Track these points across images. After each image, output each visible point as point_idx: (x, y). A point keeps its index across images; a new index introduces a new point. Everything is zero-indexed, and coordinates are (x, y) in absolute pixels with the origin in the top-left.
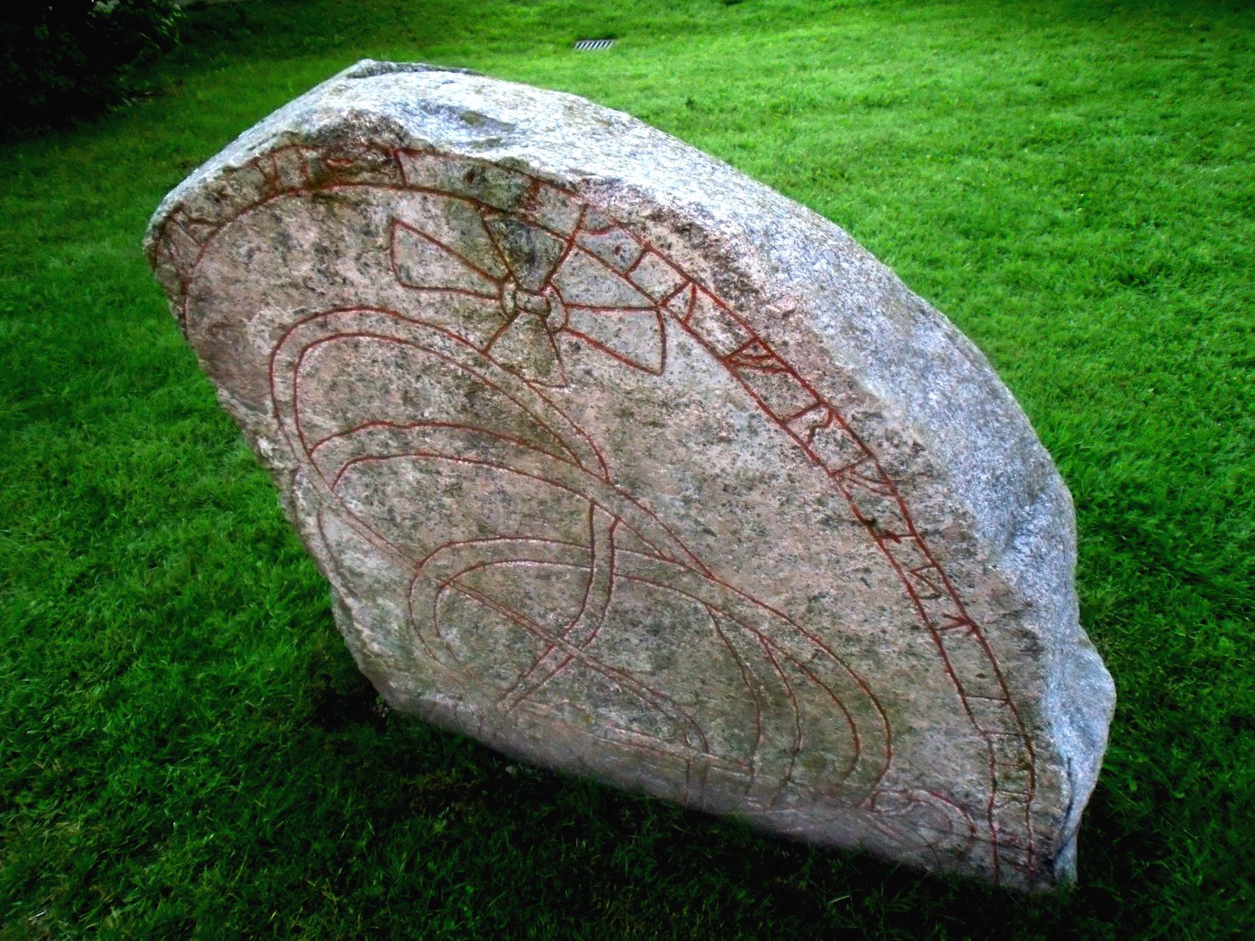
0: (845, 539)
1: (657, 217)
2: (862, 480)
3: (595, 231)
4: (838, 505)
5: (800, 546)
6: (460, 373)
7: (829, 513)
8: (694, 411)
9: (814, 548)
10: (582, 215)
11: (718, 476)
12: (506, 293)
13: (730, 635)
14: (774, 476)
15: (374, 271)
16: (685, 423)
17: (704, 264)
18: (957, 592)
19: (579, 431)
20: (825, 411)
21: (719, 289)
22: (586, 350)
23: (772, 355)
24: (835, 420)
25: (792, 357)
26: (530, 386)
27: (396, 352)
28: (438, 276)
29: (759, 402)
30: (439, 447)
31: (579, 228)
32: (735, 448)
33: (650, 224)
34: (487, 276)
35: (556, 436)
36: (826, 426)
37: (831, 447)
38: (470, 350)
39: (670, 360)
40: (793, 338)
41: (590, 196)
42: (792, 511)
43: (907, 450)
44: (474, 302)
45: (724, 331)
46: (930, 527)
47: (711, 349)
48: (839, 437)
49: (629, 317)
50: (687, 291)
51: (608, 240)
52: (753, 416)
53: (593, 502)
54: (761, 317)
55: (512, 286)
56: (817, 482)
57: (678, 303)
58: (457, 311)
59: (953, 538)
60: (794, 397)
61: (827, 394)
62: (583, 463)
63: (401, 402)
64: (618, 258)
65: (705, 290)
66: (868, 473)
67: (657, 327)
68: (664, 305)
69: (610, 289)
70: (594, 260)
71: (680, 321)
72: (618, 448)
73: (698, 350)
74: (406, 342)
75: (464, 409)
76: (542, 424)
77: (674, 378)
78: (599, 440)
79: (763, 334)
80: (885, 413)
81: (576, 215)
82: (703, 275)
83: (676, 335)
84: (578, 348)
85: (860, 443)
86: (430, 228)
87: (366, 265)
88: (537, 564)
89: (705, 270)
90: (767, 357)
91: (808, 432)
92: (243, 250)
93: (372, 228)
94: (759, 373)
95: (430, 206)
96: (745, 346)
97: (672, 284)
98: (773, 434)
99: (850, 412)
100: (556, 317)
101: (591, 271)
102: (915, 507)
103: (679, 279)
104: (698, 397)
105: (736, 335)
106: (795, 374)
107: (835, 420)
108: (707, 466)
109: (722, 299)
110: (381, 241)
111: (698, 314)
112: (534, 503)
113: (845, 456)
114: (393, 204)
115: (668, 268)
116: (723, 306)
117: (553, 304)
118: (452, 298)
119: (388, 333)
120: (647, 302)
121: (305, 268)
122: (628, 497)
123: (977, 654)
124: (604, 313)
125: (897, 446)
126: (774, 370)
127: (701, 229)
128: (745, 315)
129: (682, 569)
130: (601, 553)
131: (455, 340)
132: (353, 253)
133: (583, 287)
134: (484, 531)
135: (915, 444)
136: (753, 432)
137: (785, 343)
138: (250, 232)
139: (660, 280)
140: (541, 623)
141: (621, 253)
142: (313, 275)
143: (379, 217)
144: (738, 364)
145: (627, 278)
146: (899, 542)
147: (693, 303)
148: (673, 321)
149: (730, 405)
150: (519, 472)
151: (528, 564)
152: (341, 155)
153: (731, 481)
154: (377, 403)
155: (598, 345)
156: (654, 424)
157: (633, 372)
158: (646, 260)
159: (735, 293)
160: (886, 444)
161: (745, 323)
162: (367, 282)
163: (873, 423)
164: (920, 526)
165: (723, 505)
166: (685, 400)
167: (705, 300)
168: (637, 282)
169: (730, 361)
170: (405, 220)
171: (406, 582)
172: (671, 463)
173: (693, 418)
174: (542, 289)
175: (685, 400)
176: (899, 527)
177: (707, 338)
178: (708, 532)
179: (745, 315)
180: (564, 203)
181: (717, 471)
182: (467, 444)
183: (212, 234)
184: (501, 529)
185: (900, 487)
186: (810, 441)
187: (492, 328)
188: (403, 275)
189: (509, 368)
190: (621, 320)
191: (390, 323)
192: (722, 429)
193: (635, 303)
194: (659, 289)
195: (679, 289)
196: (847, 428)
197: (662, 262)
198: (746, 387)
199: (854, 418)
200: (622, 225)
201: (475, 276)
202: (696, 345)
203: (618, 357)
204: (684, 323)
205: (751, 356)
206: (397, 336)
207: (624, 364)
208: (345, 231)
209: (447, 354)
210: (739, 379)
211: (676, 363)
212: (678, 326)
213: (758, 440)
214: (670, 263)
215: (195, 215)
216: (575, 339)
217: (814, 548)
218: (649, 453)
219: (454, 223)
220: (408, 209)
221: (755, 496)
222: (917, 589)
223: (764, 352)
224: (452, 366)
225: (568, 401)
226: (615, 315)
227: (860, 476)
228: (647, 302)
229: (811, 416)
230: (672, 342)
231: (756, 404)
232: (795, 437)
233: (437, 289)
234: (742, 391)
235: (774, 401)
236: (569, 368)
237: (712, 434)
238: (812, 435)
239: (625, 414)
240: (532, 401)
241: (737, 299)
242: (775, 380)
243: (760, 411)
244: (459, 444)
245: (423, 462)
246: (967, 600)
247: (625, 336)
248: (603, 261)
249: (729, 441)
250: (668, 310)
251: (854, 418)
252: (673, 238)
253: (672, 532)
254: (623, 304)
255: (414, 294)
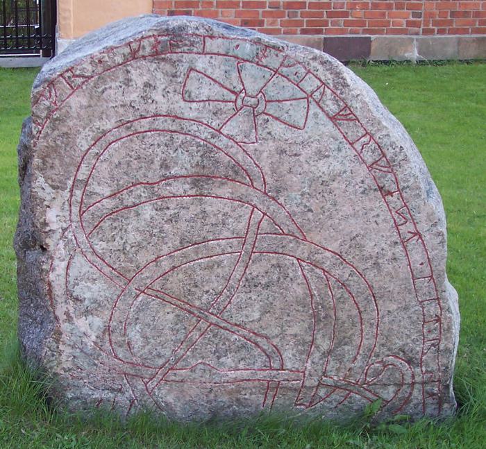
0: (370, 200)
1: (314, 59)
2: (380, 168)
3: (288, 66)
4: (370, 182)
5: (351, 208)
6: (202, 144)
7: (366, 186)
8: (315, 145)
9: (357, 208)
10: (284, 60)
11: (321, 176)
12: (239, 98)
13: (308, 276)
14: (345, 172)
15: (171, 95)
16: (310, 152)
17: (330, 76)
18: (414, 217)
19: (257, 166)
20: (368, 136)
21: (334, 86)
22: (270, 122)
23: (352, 113)
24: (372, 140)
25: (358, 114)
26: (238, 145)
27: (168, 138)
28: (206, 94)
29: (344, 136)
30: (174, 191)
31: (281, 65)
32: (331, 159)
33: (311, 62)
34: (233, 92)
35: (245, 171)
36: (368, 144)
37: (370, 154)
38: (211, 130)
39: (308, 121)
40: (358, 105)
41: (288, 52)
42: (351, 189)
43: (398, 150)
44: (222, 105)
45: (334, 104)
46: (405, 185)
47: (327, 115)
48: (373, 148)
49: (294, 102)
50: (322, 89)
51: (293, 69)
52: (341, 143)
53: (254, 207)
54: (350, 97)
55: (243, 95)
56: (362, 171)
57: (317, 94)
58: (210, 111)
59: (413, 189)
60: (357, 131)
61: (369, 129)
62: (255, 184)
63: (159, 168)
64: (295, 77)
65: (328, 87)
66: (383, 164)
67: (306, 106)
68: (311, 96)
69: (290, 90)
70: (285, 79)
71: (316, 102)
72: (274, 172)
73: (321, 114)
74: (175, 132)
75: (197, 165)
76: (239, 165)
77: (308, 130)
78: (267, 169)
79: (349, 104)
80: (391, 135)
81: (281, 60)
82: (329, 81)
83: (314, 109)
84: (268, 121)
85: (381, 150)
86: (208, 73)
87: (168, 92)
88: (209, 259)
89: (329, 77)
90: (349, 114)
91: (361, 148)
92: (100, 90)
93: (178, 73)
94: (345, 122)
95: (212, 61)
96: (341, 111)
97: (316, 86)
98: (347, 150)
99: (377, 136)
100: (261, 108)
101: (282, 84)
102: (400, 176)
103: (319, 84)
104: (318, 138)
105: (339, 105)
106: (359, 122)
107: (372, 140)
108: (316, 172)
109: (335, 91)
110: (180, 80)
111: (324, 98)
112: (220, 216)
113: (374, 157)
114: (194, 62)
115: (315, 79)
116: (335, 93)
117: (260, 102)
118: (209, 104)
119: (166, 128)
120: (305, 95)
121: (134, 96)
122: (274, 199)
123: (420, 250)
124: (284, 102)
125: (394, 149)
126: (350, 120)
127: (330, 62)
128: (343, 96)
129: (292, 238)
130: (250, 240)
131: (204, 126)
132: (163, 86)
133: (276, 92)
134: (184, 242)
135: (401, 147)
136: (339, 150)
137: (356, 108)
138: (108, 80)
139: (310, 84)
140: (197, 303)
141: (298, 74)
142: (137, 99)
143: (183, 68)
144: (336, 119)
145: (297, 85)
146: (392, 196)
147: (323, 94)
148: (313, 103)
149: (332, 139)
150: (216, 197)
151: (202, 261)
152: (179, 38)
153: (326, 178)
154: (143, 171)
155: (277, 119)
156: (296, 155)
157: (291, 130)
158: (307, 77)
159: (340, 87)
160: (390, 148)
161: (343, 100)
162: (165, 101)
163: (385, 140)
164: (402, 184)
165: (320, 193)
166: (312, 140)
167: (328, 92)
168: (301, 87)
169: (333, 119)
170: (198, 69)
171: (115, 297)
172: (300, 174)
173: (313, 148)
174: (257, 95)
175: (312, 140)
176: (393, 187)
177: (326, 109)
178: (310, 210)
179: (343, 96)
180: (277, 55)
181: (321, 174)
182: (193, 186)
183: (83, 83)
184: (195, 239)
185: (395, 168)
186: (361, 152)
187: (227, 117)
188: (186, 96)
189: (229, 137)
190: (291, 105)
191: (169, 122)
192: (326, 150)
193: (298, 96)
194: (309, 89)
195: (318, 88)
196: (376, 143)
197: (314, 77)
198: (339, 129)
199: (379, 138)
200: (299, 63)
201: (225, 92)
202: (321, 112)
203: (285, 124)
204: (318, 103)
205: (342, 115)
206: (171, 128)
207: (287, 126)
208: (162, 75)
209: (198, 134)
210: (336, 126)
211: (310, 122)
212: (315, 104)
213: (340, 154)
214: (316, 77)
215: (78, 72)
216: (266, 117)
217: (357, 208)
218: (290, 172)
219: (222, 67)
220: (201, 63)
221: (335, 184)
222: (397, 220)
223: (349, 112)
224: (199, 140)
225: (256, 150)
226: (288, 103)
227: (379, 166)
228: (305, 95)
229: (363, 139)
230: (311, 112)
231: (342, 136)
232: (356, 150)
233: (203, 101)
234: (338, 131)
235: (350, 134)
236: (260, 133)
237: (321, 155)
238: (362, 149)
239: (283, 152)
240: (237, 153)
241: (341, 90)
242: (351, 124)
243: (344, 140)
244: (187, 186)
245: (160, 203)
246: (418, 221)
247: (291, 112)
248: (288, 79)
249: (328, 156)
250: (312, 98)
251: (379, 138)
252: (320, 67)
253: (291, 216)
254: (294, 97)
255: (189, 104)
